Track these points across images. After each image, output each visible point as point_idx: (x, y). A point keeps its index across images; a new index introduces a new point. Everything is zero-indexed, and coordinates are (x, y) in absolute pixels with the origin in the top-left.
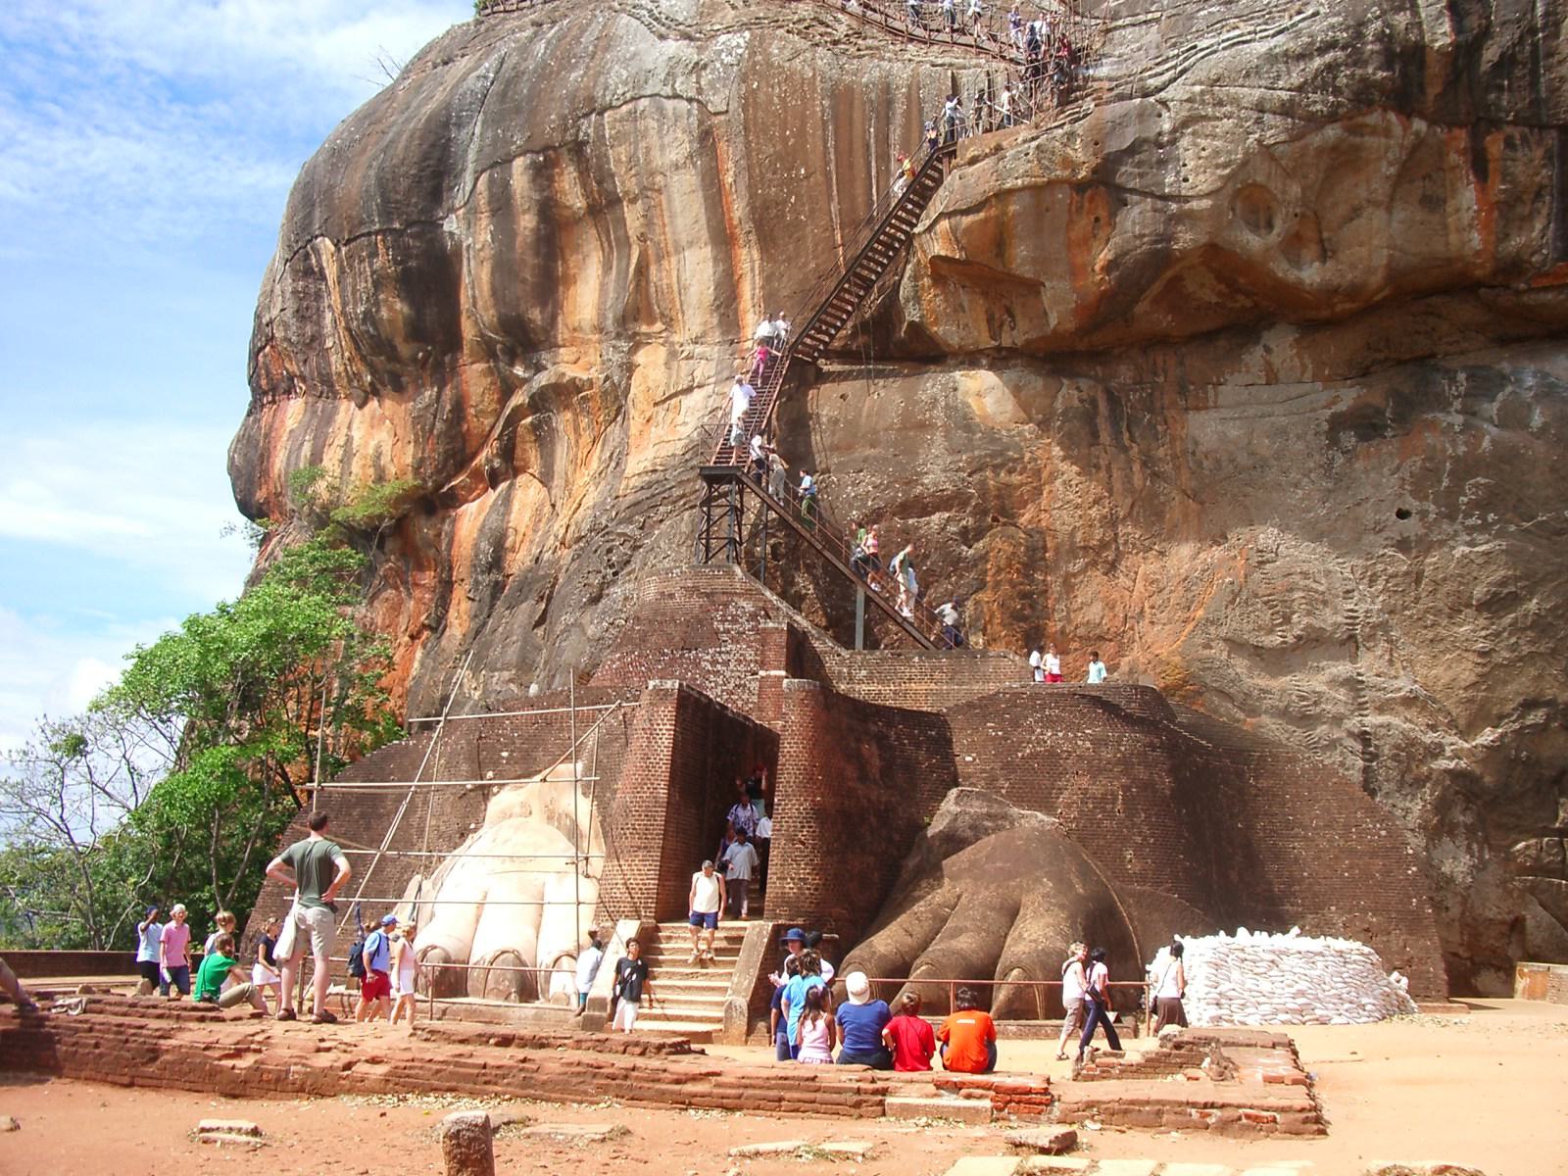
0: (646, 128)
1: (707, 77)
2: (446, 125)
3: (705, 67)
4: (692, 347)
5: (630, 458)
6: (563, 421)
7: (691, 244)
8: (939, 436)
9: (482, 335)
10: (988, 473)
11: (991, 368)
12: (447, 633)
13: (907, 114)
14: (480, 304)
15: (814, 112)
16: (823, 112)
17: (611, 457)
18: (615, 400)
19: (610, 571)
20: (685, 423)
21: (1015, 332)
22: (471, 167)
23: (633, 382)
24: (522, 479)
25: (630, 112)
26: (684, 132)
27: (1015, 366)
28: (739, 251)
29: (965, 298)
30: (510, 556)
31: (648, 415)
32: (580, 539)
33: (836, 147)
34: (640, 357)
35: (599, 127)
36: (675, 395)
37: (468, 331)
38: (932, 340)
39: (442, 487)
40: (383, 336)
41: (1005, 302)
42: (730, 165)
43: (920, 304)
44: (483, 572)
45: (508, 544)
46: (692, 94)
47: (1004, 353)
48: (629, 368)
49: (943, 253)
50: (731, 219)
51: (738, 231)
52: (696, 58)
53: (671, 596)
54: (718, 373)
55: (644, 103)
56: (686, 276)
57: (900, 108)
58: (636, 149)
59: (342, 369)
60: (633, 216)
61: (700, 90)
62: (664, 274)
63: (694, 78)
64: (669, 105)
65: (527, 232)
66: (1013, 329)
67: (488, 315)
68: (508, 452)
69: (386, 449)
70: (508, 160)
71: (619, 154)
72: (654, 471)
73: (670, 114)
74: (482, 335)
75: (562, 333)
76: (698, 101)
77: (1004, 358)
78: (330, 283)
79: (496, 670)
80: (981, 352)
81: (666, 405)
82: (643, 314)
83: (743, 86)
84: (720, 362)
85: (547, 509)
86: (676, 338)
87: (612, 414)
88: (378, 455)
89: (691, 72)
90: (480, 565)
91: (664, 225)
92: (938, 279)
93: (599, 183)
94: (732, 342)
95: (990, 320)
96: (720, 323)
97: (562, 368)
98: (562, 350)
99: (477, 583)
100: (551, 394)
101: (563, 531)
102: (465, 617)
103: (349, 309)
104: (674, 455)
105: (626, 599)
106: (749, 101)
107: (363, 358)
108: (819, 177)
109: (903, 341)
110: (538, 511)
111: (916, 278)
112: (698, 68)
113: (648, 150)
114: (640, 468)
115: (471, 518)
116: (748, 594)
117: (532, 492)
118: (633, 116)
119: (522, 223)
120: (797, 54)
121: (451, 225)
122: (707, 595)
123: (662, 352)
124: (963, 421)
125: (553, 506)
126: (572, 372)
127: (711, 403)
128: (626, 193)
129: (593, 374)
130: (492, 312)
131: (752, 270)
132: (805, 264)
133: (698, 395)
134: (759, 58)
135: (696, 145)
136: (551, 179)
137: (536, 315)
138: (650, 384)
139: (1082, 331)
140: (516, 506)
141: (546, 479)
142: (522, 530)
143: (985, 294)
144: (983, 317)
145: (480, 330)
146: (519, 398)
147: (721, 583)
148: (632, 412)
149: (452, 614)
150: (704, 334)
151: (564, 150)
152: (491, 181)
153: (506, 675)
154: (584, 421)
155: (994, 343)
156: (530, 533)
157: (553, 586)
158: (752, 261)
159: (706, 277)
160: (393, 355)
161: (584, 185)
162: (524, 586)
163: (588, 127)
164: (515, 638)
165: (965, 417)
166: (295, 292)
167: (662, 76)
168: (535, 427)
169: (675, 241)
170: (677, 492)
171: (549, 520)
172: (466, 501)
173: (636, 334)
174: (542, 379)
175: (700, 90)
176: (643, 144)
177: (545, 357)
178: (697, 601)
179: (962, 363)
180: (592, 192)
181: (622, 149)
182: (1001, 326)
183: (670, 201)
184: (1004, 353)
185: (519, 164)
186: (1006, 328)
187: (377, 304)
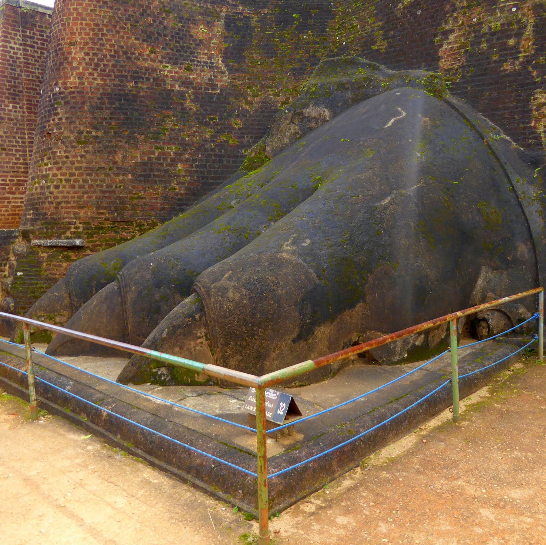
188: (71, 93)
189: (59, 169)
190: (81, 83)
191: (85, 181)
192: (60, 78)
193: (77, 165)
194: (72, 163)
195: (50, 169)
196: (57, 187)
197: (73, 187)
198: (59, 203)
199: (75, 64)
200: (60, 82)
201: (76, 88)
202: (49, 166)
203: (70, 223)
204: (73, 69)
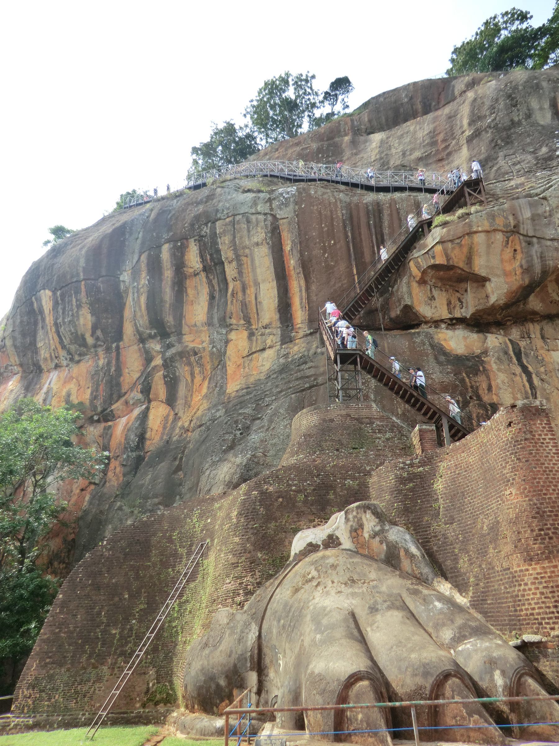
0: (240, 228)
1: (275, 204)
2: (123, 234)
3: (274, 199)
4: (263, 330)
5: (228, 385)
6: (183, 371)
7: (264, 281)
8: (431, 359)
9: (138, 331)
10: (464, 375)
11: (447, 328)
12: (108, 484)
13: (391, 215)
14: (139, 314)
15: (338, 216)
16: (343, 215)
17: (216, 386)
18: (220, 358)
19: (238, 433)
20: (263, 365)
21: (462, 310)
22: (137, 251)
23: (228, 348)
24: (153, 404)
25: (230, 222)
26: (262, 228)
27: (459, 329)
28: (292, 283)
29: (436, 293)
30: (148, 443)
31: (238, 363)
32: (200, 426)
33: (352, 230)
34: (233, 336)
35: (213, 229)
36: (255, 352)
37: (128, 330)
38: (416, 315)
39: (106, 409)
40: (79, 333)
41: (458, 295)
42: (289, 242)
43: (413, 293)
44: (132, 451)
45: (148, 435)
46: (268, 211)
47: (454, 321)
48: (227, 342)
49: (437, 262)
50: (289, 267)
51: (292, 272)
52: (269, 196)
53: (332, 421)
54: (282, 340)
55: (238, 218)
56: (261, 297)
57: (386, 213)
58: (234, 237)
59: (47, 355)
60: (230, 271)
61: (272, 209)
62: (247, 296)
63: (268, 204)
64: (253, 218)
65: (169, 279)
66: (462, 308)
67: (143, 320)
68: (147, 390)
69: (74, 392)
70: (159, 247)
71: (224, 240)
72: (249, 388)
73: (254, 220)
74: (138, 331)
75: (185, 329)
76: (272, 215)
77: (453, 325)
78: (46, 312)
79: (149, 498)
80: (442, 321)
81: (250, 358)
82: (234, 315)
83: (297, 207)
84: (282, 335)
85: (171, 418)
86: (253, 327)
87: (216, 365)
88: (69, 395)
89: (266, 202)
90: (130, 447)
91: (248, 273)
92: (422, 282)
93: (211, 255)
94: (288, 326)
95: (449, 303)
96: (280, 318)
97: (186, 344)
98: (184, 336)
99: (128, 456)
100: (178, 358)
101: (186, 425)
102: (121, 475)
103: (60, 320)
104: (259, 380)
105: (262, 441)
106: (299, 214)
107: (64, 347)
108: (342, 243)
109: (397, 317)
110: (166, 418)
111: (408, 283)
112: (270, 200)
113: (241, 238)
114: (238, 387)
115: (122, 426)
116: (381, 419)
117: (161, 409)
118: (233, 223)
119: (166, 275)
120: (324, 194)
121: (125, 277)
122: (356, 419)
123: (245, 334)
124: (440, 351)
125: (176, 414)
126: (191, 345)
127: (283, 352)
128: (227, 258)
129: (204, 345)
130: (146, 318)
131: (301, 291)
132: (334, 285)
133: (270, 353)
134: (304, 195)
135: (269, 235)
136: (183, 255)
137: (169, 319)
138: (240, 348)
139: (507, 306)
140: (151, 416)
141: (171, 401)
142: (155, 427)
143: (447, 291)
144: (445, 302)
145: (137, 328)
146: (158, 361)
147: (364, 413)
148: (228, 363)
149: (110, 474)
150: (270, 323)
151: (192, 240)
152: (149, 256)
153: (156, 500)
154: (197, 370)
155: (450, 316)
156: (161, 429)
157: (183, 452)
158: (300, 287)
159: (272, 295)
160: (83, 343)
161: (202, 256)
162: (162, 453)
163: (206, 230)
164: (160, 480)
165: (441, 349)
166: (22, 322)
167: (250, 205)
168: (165, 377)
169: (255, 280)
170: (275, 391)
171: (173, 422)
172: (119, 417)
173: (231, 325)
174: (173, 351)
175: (272, 209)
176: (238, 235)
177: (173, 339)
178: (348, 421)
179: (431, 327)
180: (206, 260)
181: (226, 238)
182: (454, 307)
183: (253, 261)
184: (454, 321)
185: (166, 248)
186: (458, 308)
187: (78, 316)
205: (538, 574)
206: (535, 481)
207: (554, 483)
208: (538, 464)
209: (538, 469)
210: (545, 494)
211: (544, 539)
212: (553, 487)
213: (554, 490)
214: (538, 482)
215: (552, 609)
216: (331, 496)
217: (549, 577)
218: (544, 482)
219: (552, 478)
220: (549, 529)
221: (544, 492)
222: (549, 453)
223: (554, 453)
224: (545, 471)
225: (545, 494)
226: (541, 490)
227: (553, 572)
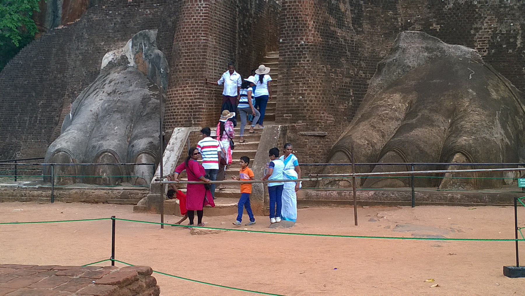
188: (311, 45)
189: (311, 90)
190: (314, 40)
191: (323, 98)
192: (304, 36)
193: (319, 88)
194: (317, 87)
195: (305, 90)
196: (311, 101)
197: (318, 101)
198: (313, 111)
199: (310, 28)
200: (304, 38)
201: (313, 42)
202: (305, 88)
203: (318, 122)
204: (310, 31)
205: (170, 95)
206: (183, 30)
207: (196, 32)
208: (189, 16)
209: (188, 20)
210: (187, 40)
211: (177, 72)
212: (194, 35)
213: (193, 37)
214: (185, 31)
215: (170, 117)
216: (132, 24)
217: (174, 97)
218: (189, 31)
219: (196, 28)
220: (181, 65)
221: (187, 38)
222: (200, 7)
223: (203, 7)
224: (192, 22)
225: (187, 40)
226: (185, 37)
227: (175, 94)
